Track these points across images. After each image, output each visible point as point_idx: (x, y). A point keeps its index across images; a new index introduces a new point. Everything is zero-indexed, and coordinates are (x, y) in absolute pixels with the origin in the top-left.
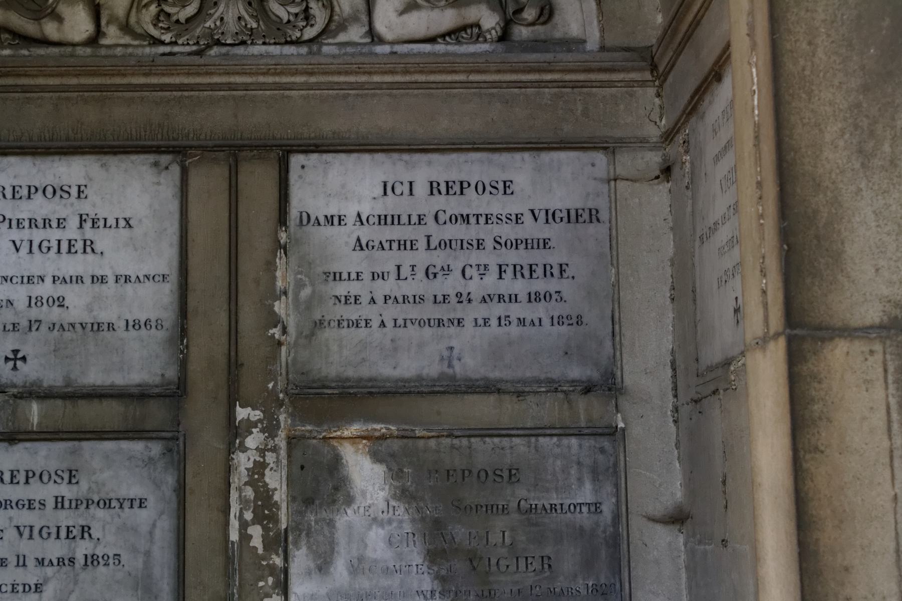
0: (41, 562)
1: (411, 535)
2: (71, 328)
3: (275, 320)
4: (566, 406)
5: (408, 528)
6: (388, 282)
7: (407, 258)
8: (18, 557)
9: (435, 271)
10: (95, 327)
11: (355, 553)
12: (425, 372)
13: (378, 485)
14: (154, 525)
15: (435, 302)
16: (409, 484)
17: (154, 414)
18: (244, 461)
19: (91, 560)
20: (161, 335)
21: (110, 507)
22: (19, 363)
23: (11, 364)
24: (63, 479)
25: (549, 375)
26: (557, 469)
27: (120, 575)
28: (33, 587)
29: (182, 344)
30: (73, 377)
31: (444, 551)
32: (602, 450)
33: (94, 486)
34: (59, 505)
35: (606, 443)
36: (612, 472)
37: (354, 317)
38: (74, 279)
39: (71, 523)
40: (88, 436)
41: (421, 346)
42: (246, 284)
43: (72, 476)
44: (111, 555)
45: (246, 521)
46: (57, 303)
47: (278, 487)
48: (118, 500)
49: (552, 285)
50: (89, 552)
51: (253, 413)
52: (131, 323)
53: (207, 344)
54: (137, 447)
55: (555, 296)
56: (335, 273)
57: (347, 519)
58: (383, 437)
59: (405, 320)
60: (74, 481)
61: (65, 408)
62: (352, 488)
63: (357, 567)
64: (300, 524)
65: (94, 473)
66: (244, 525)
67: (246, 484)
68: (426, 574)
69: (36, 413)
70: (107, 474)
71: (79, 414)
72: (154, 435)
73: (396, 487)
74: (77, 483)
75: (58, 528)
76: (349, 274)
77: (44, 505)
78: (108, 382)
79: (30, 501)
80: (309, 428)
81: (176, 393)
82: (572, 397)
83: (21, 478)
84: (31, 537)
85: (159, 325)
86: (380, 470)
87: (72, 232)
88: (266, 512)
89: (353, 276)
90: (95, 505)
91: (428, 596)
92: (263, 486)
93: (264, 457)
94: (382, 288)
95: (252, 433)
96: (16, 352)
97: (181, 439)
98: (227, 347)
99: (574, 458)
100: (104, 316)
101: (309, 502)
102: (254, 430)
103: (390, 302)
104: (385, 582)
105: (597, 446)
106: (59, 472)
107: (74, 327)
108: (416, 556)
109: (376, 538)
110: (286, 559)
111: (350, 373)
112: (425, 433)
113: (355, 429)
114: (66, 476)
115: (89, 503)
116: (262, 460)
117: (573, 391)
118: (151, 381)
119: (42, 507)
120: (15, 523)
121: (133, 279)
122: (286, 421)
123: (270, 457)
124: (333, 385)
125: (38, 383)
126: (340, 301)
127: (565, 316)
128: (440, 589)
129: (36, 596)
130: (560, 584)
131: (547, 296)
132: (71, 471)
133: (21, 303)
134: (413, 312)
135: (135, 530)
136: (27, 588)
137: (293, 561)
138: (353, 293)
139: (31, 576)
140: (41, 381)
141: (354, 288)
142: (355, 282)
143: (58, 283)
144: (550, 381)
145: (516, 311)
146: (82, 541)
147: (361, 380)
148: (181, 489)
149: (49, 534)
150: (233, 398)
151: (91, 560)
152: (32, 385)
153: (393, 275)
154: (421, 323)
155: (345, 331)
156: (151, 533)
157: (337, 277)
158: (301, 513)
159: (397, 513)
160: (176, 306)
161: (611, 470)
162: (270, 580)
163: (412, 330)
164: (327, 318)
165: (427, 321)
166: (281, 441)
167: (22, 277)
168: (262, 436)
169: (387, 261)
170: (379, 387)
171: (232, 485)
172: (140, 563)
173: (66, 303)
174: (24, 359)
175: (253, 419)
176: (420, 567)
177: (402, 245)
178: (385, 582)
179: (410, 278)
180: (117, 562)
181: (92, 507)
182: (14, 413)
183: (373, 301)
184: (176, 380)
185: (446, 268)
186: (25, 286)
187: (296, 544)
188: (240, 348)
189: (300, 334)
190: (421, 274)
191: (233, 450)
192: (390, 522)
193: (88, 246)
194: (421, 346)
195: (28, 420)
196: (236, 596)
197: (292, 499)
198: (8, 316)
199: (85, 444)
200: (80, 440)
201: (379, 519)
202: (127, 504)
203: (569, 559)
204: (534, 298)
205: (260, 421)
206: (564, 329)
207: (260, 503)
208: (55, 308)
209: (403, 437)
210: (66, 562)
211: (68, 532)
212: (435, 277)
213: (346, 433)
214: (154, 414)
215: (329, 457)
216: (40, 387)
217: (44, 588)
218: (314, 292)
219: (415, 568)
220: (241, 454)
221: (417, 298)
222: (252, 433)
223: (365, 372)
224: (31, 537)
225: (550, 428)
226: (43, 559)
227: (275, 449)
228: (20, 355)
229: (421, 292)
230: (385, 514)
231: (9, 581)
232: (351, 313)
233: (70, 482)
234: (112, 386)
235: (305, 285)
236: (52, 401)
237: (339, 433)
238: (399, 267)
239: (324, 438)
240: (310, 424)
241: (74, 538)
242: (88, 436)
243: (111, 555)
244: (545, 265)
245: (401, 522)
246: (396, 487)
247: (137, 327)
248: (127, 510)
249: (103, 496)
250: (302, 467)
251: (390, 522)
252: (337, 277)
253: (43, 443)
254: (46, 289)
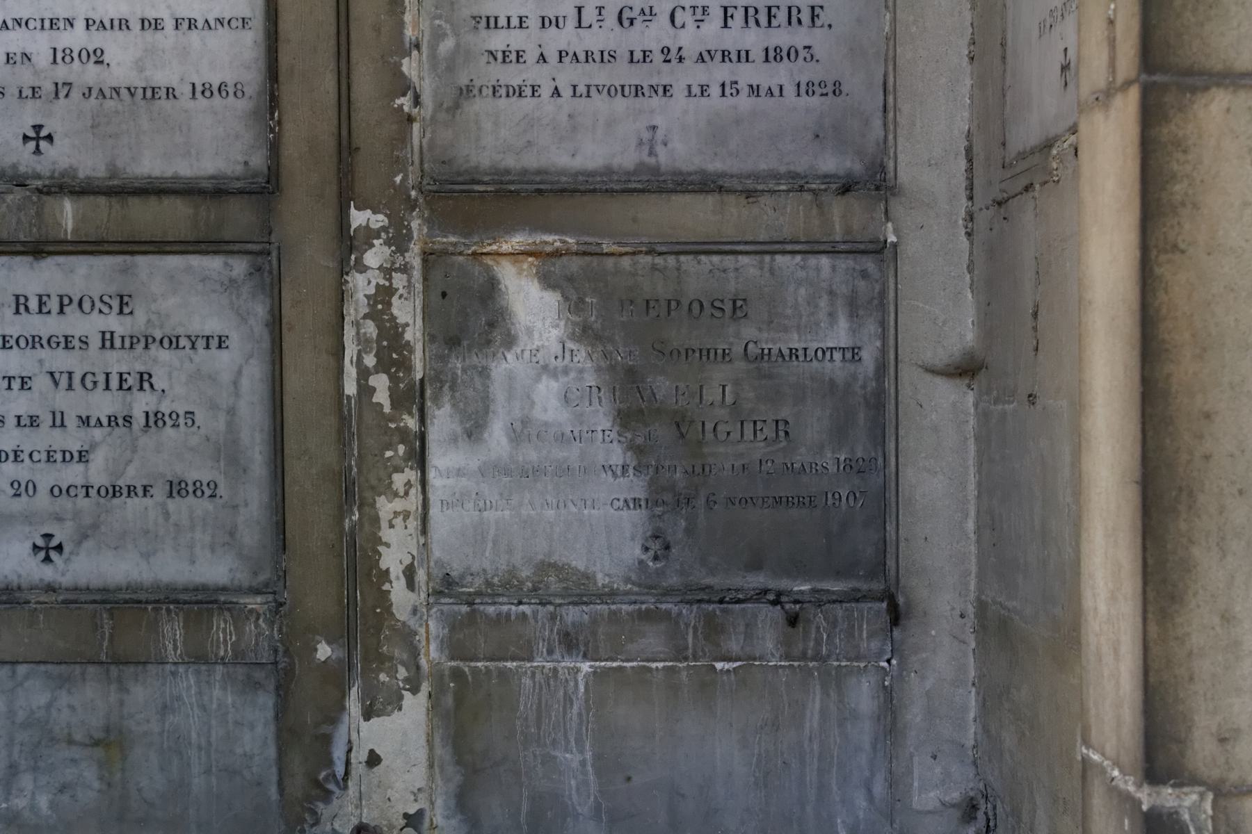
0: (85, 421)
1: (595, 390)
2: (114, 95)
3: (404, 86)
4: (815, 211)
5: (591, 380)
6: (564, 31)
8: (54, 413)
9: (632, 16)
10: (149, 93)
11: (517, 413)
12: (616, 162)
13: (549, 320)
14: (240, 372)
15: (632, 61)
16: (593, 319)
17: (233, 217)
18: (362, 285)
20: (242, 105)
21: (177, 347)
22: (43, 144)
23: (32, 145)
24: (111, 307)
25: (792, 168)
26: (800, 299)
27: (194, 441)
28: (76, 455)
29: (272, 118)
30: (120, 164)
31: (641, 411)
32: (864, 274)
33: (154, 317)
34: (108, 344)
35: (869, 264)
36: (877, 304)
37: (515, 82)
38: (116, 23)
39: (124, 369)
40: (143, 248)
41: (611, 123)
42: (361, 33)
43: (124, 304)
44: (181, 413)
45: (366, 367)
46: (93, 58)
47: (411, 322)
48: (189, 337)
49: (799, 37)
50: (151, 409)
51: (374, 218)
52: (199, 89)
53: (309, 120)
54: (213, 264)
55: (803, 53)
56: (488, 18)
57: (507, 367)
58: (557, 254)
59: (588, 86)
60: (126, 310)
61: (111, 207)
62: (513, 324)
63: (521, 432)
64: (441, 372)
65: (155, 301)
66: (364, 373)
67: (366, 317)
68: (615, 443)
69: (70, 216)
70: (172, 301)
71: (130, 217)
72: (237, 247)
73: (575, 324)
74: (131, 313)
75: (107, 375)
76: (509, 18)
77: (86, 343)
78: (169, 173)
79: (66, 337)
80: (452, 239)
81: (266, 188)
82: (824, 198)
83: (54, 305)
84: (70, 387)
85: (239, 92)
86: (552, 299)
88: (394, 356)
89: (514, 22)
90: (157, 343)
91: (619, 473)
92: (388, 321)
93: (390, 279)
95: (372, 246)
96: (38, 128)
97: (274, 254)
98: (336, 122)
99: (824, 285)
100: (162, 78)
101: (453, 342)
102: (375, 242)
103: (567, 60)
104: (559, 453)
105: (858, 267)
106: (106, 299)
107: (118, 93)
108: (601, 418)
109: (547, 393)
110: (422, 420)
111: (510, 162)
112: (615, 248)
113: (517, 241)
114: (115, 304)
115: (148, 341)
116: (387, 284)
117: (825, 190)
118: (229, 172)
119: (84, 346)
120: (47, 367)
121: (200, 24)
122: (420, 230)
123: (399, 280)
124: (486, 179)
125: (71, 172)
126: (496, 59)
127: (816, 83)
128: (634, 463)
129: (81, 467)
130: (802, 456)
131: (792, 54)
132: (121, 297)
133: (42, 58)
134: (601, 75)
135: (213, 378)
136: (68, 456)
137: (432, 423)
138: (513, 48)
139: (73, 439)
140: (75, 170)
142: (518, 31)
143: (93, 28)
144: (793, 176)
145: (747, 74)
146: (142, 393)
147: (525, 172)
148: (276, 324)
149: (95, 383)
150: (345, 197)
151: (154, 420)
152: (63, 175)
153: (572, 22)
154: (611, 91)
155: (503, 102)
156: (236, 383)
157: (491, 23)
158: (443, 358)
159: (576, 359)
160: (262, 64)
161: (876, 302)
162: (401, 449)
163: (599, 101)
164: (477, 83)
165: (619, 89)
166: (414, 258)
167: (42, 20)
168: (387, 251)
170: (552, 183)
171: (347, 319)
172: (221, 425)
173: (106, 58)
174: (49, 138)
175: (375, 226)
176: (607, 433)
178: (559, 453)
179: (596, 26)
180: (190, 423)
181: (153, 347)
182: (39, 214)
183: (543, 58)
184: (265, 170)
185: (647, 11)
186: (46, 34)
187: (436, 399)
188: (354, 125)
189: (439, 106)
190: (611, 20)
191: (347, 269)
192: (566, 371)
194: (611, 123)
195: (60, 225)
196: (355, 470)
197: (430, 338)
198: (25, 77)
199: (140, 259)
200: (132, 253)
201: (551, 367)
202: (201, 343)
203: (813, 424)
204: (773, 55)
205: (384, 229)
206: (815, 101)
207: (385, 343)
208: (91, 65)
209: (585, 254)
210: (120, 421)
211: (121, 380)
212: (632, 24)
213: (505, 248)
214: (233, 217)
215: (481, 280)
216: (74, 177)
217: (92, 457)
218: (458, 45)
219: (601, 434)
220: (357, 275)
221: (606, 54)
222: (372, 246)
223: (531, 161)
224: (70, 387)
225: (791, 242)
226: (88, 417)
227: (405, 269)
228: (43, 133)
229: (611, 46)
230: (560, 359)
231: (42, 447)
232: (512, 75)
233: (121, 312)
234: (176, 178)
235: (445, 35)
236: (92, 198)
237: (494, 247)
238: (580, 9)
239: (474, 254)
240: (454, 234)
241: (129, 389)
242: (143, 248)
243: (181, 413)
244: (790, 8)
245: (581, 371)
246: (575, 324)
247: (208, 94)
248: (201, 351)
249: (168, 331)
250: (444, 295)
251: (566, 371)
252: (491, 23)
253: (82, 258)
254: (76, 38)
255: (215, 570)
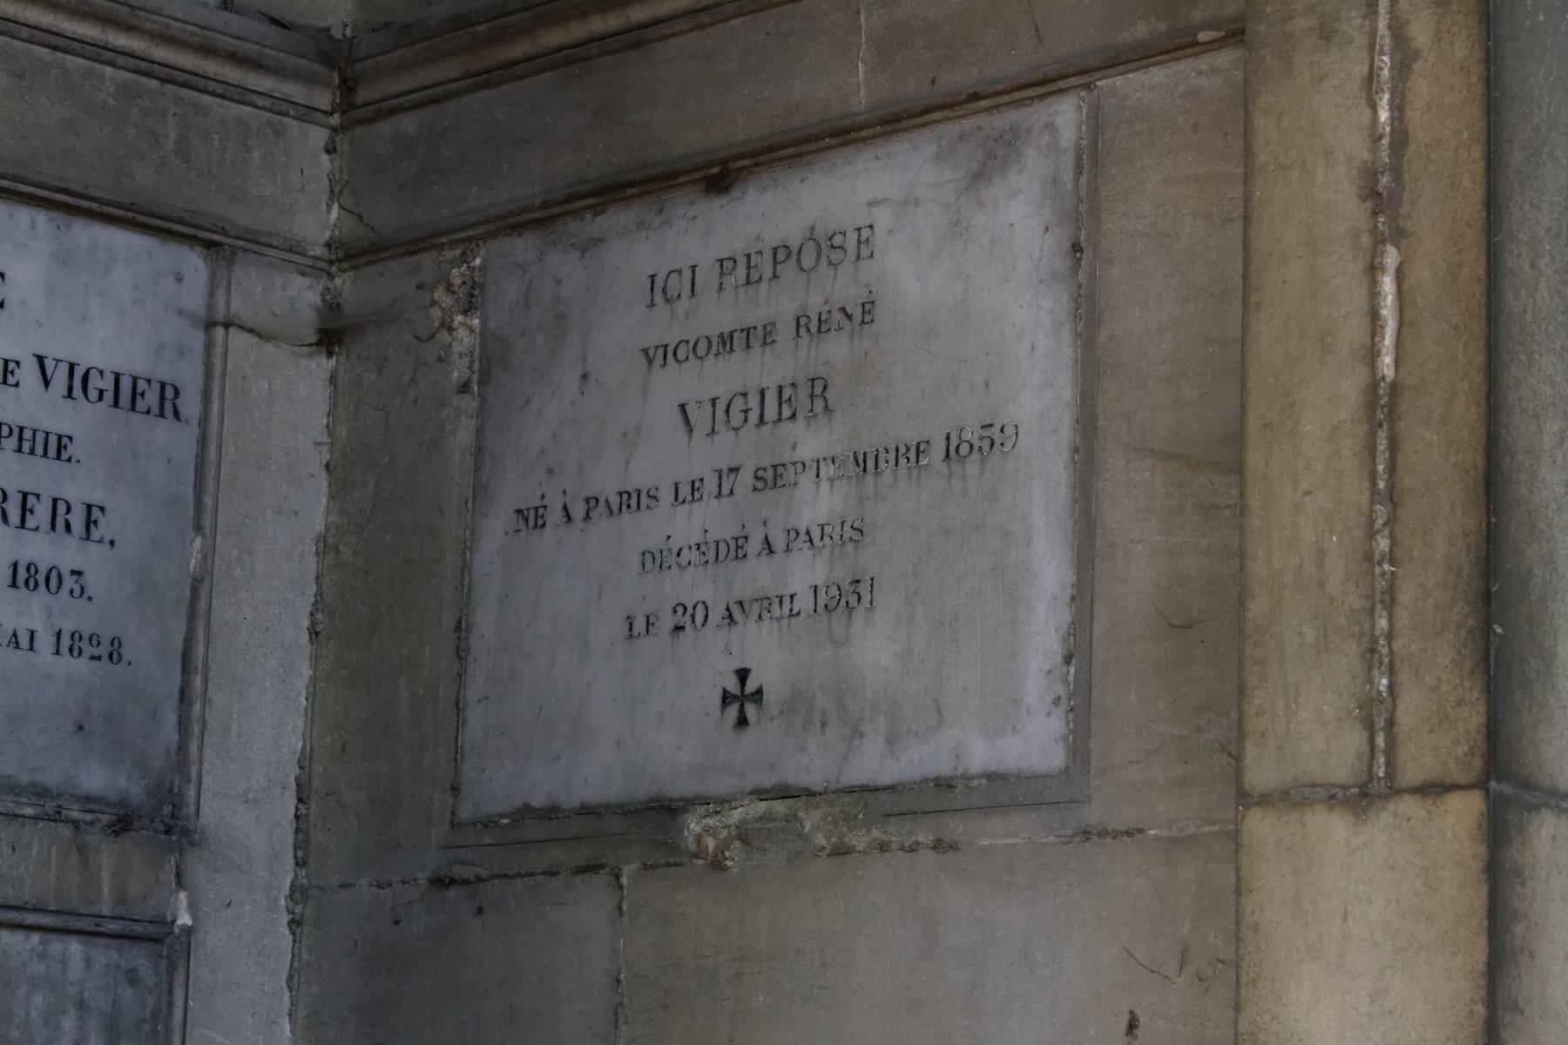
4: (74, 859)
25: (39, 778)
32: (133, 978)
49: (65, 553)
55: (69, 582)
82: (93, 838)
99: (71, 990)
105: (123, 965)
117: (92, 823)
127: (86, 636)
131: (52, 579)
144: (40, 792)
161: (146, 1027)
206: (81, 666)
244: (55, 501)
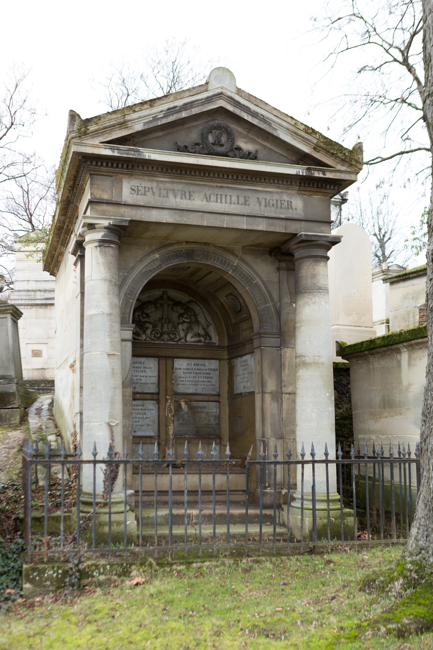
7: (191, 375)
17: (155, 397)
18: (168, 404)
19: (146, 418)
43: (143, 405)
49: (211, 380)
54: (152, 401)
81: (158, 394)
87: (142, 369)
94: (187, 379)
100: (147, 382)
130: (211, 423)
134: (191, 383)
139: (138, 420)
141: (183, 379)
148: (159, 408)
150: (166, 395)
151: (146, 418)
157: (181, 377)
169: (188, 375)
177: (190, 373)
193: (145, 371)
203: (212, 420)
204: (208, 382)
232: (182, 383)
252: (181, 377)
254: (139, 378)
255: (152, 434)
